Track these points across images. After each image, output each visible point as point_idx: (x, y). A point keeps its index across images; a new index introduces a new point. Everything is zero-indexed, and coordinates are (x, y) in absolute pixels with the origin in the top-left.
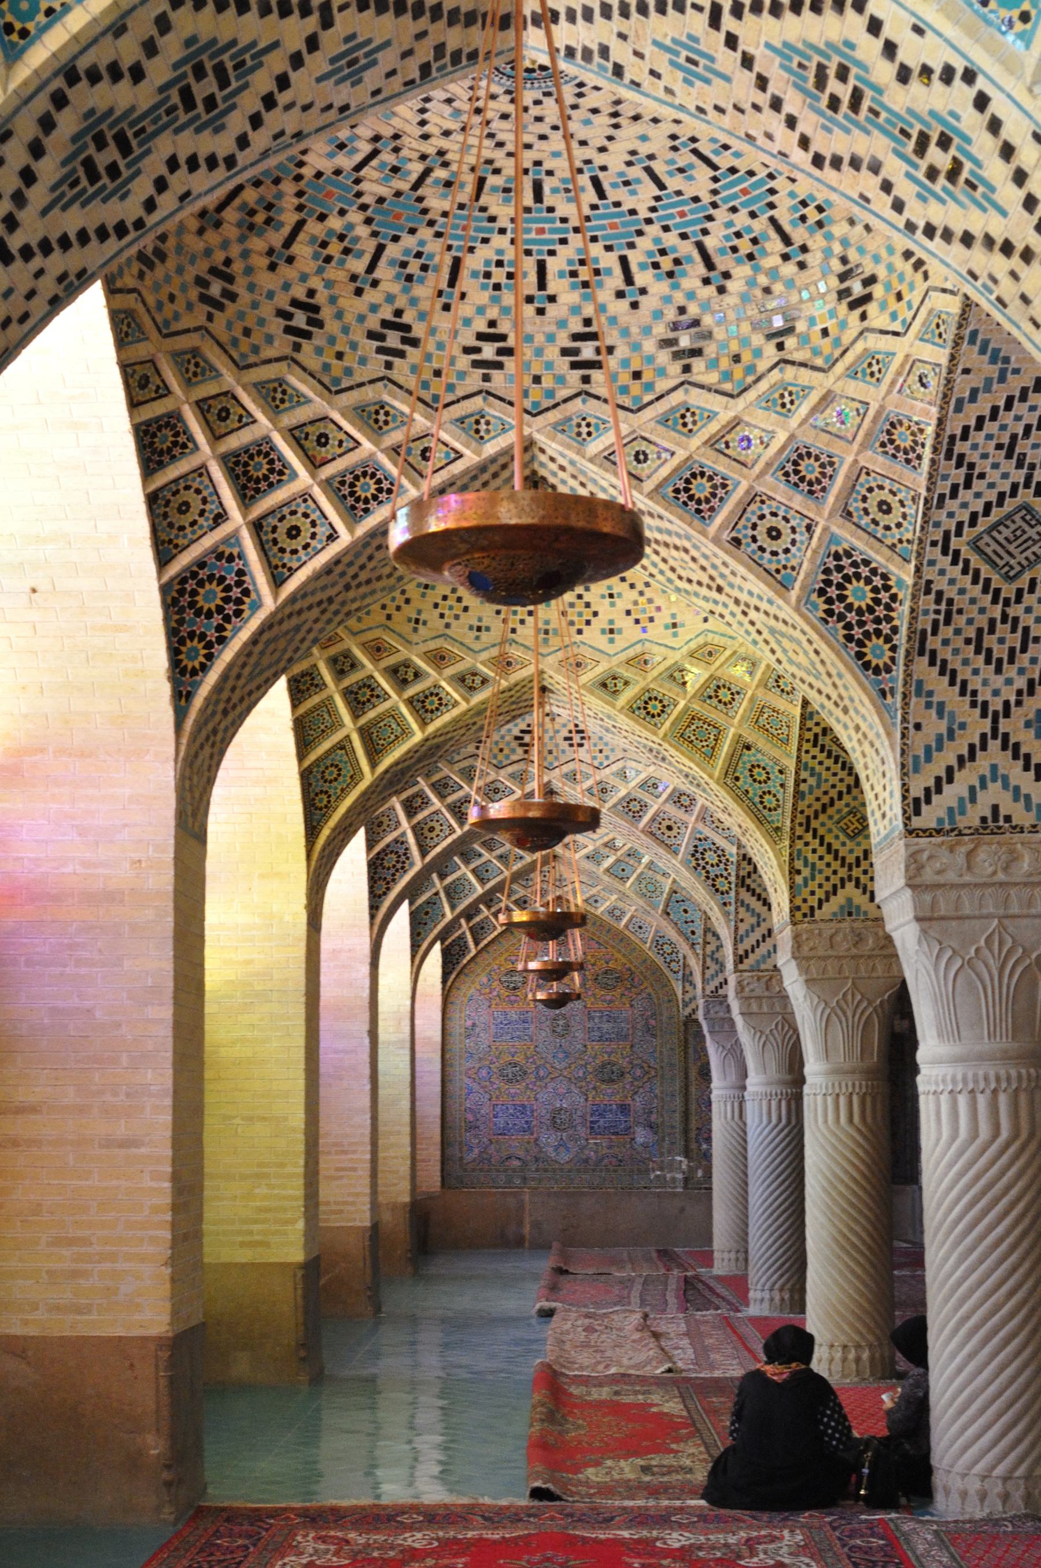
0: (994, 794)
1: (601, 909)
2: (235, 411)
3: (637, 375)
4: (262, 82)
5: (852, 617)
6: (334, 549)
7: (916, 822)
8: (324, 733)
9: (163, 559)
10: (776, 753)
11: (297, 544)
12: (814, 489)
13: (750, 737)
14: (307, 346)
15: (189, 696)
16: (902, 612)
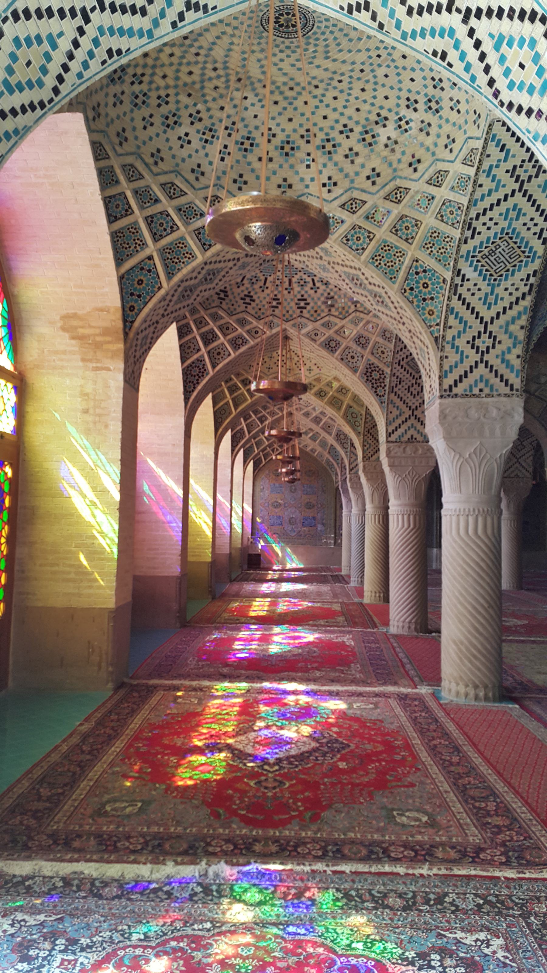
0: (412, 432)
1: (308, 449)
2: (204, 321)
3: (316, 311)
4: (223, 273)
5: (373, 381)
6: (230, 358)
7: (390, 439)
8: (221, 400)
9: (183, 362)
10: (359, 409)
11: (220, 357)
12: (364, 346)
13: (352, 404)
14: (224, 302)
15: (189, 399)
16: (387, 381)
